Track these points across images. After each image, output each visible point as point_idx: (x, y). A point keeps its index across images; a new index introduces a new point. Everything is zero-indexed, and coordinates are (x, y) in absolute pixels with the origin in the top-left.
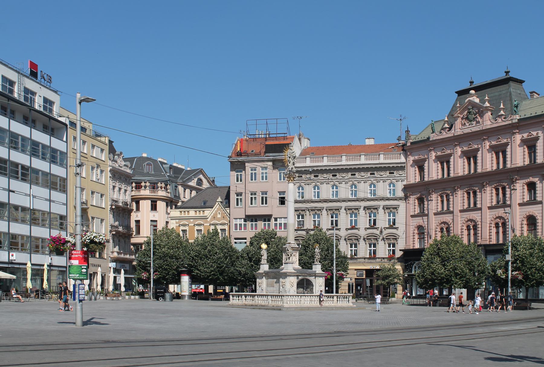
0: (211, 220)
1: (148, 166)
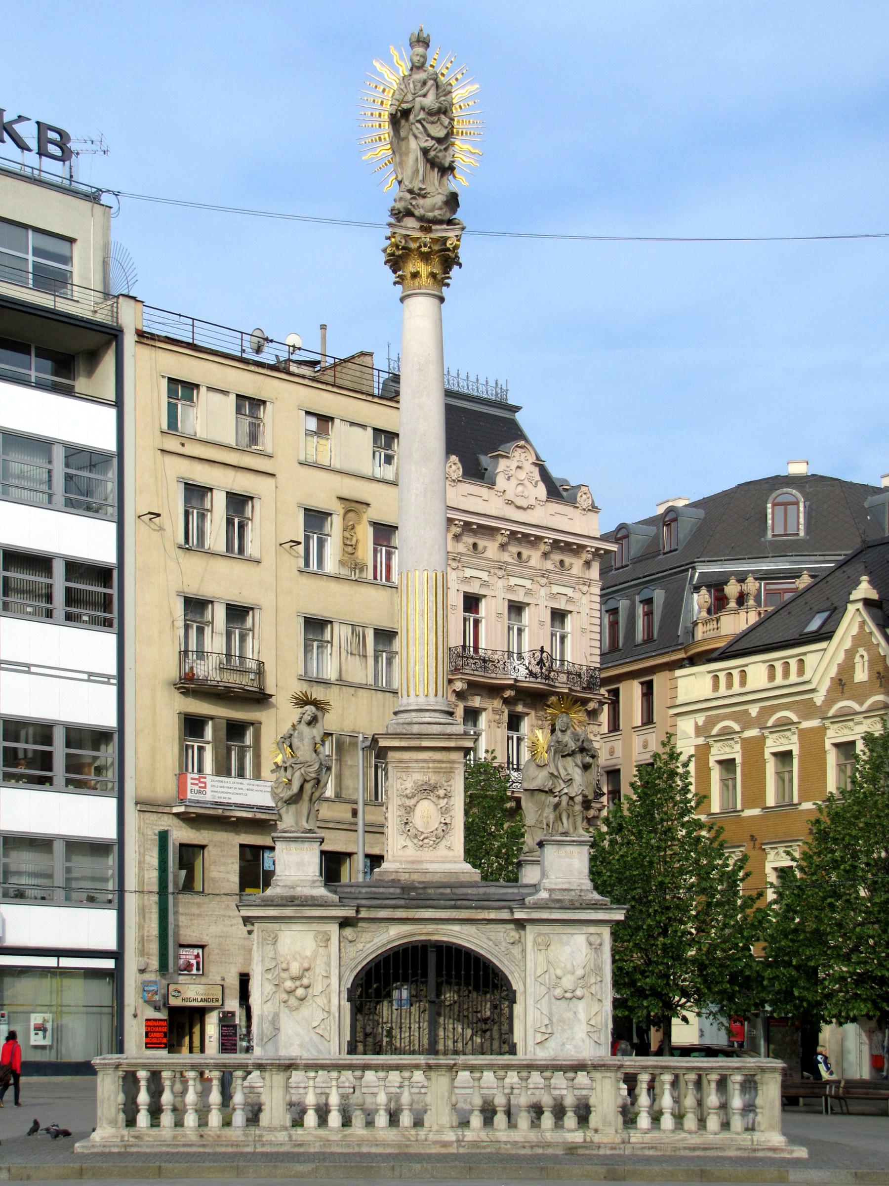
0: (830, 700)
1: (780, 510)
